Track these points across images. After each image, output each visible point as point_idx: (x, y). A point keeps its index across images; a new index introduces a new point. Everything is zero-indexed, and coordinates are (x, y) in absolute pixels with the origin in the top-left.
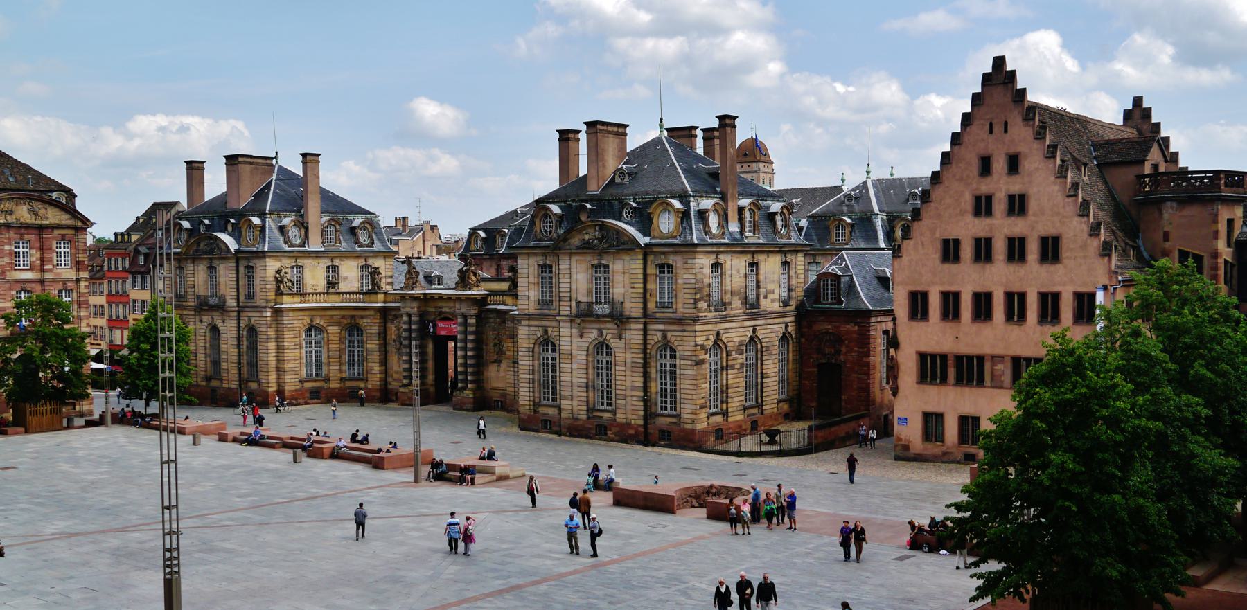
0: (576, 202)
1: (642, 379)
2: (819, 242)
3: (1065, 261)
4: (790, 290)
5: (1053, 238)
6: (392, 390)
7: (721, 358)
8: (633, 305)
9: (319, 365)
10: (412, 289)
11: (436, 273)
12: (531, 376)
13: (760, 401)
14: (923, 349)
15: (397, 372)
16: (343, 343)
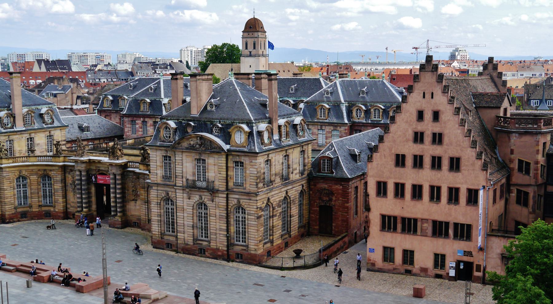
0: (184, 120)
1: (226, 225)
2: (311, 117)
3: (463, 171)
4: (304, 166)
5: (456, 158)
6: (70, 212)
7: (270, 211)
8: (220, 183)
9: (25, 197)
10: (82, 157)
11: (85, 125)
12: (159, 218)
13: (289, 230)
14: (384, 213)
15: (73, 202)
16: (40, 185)
